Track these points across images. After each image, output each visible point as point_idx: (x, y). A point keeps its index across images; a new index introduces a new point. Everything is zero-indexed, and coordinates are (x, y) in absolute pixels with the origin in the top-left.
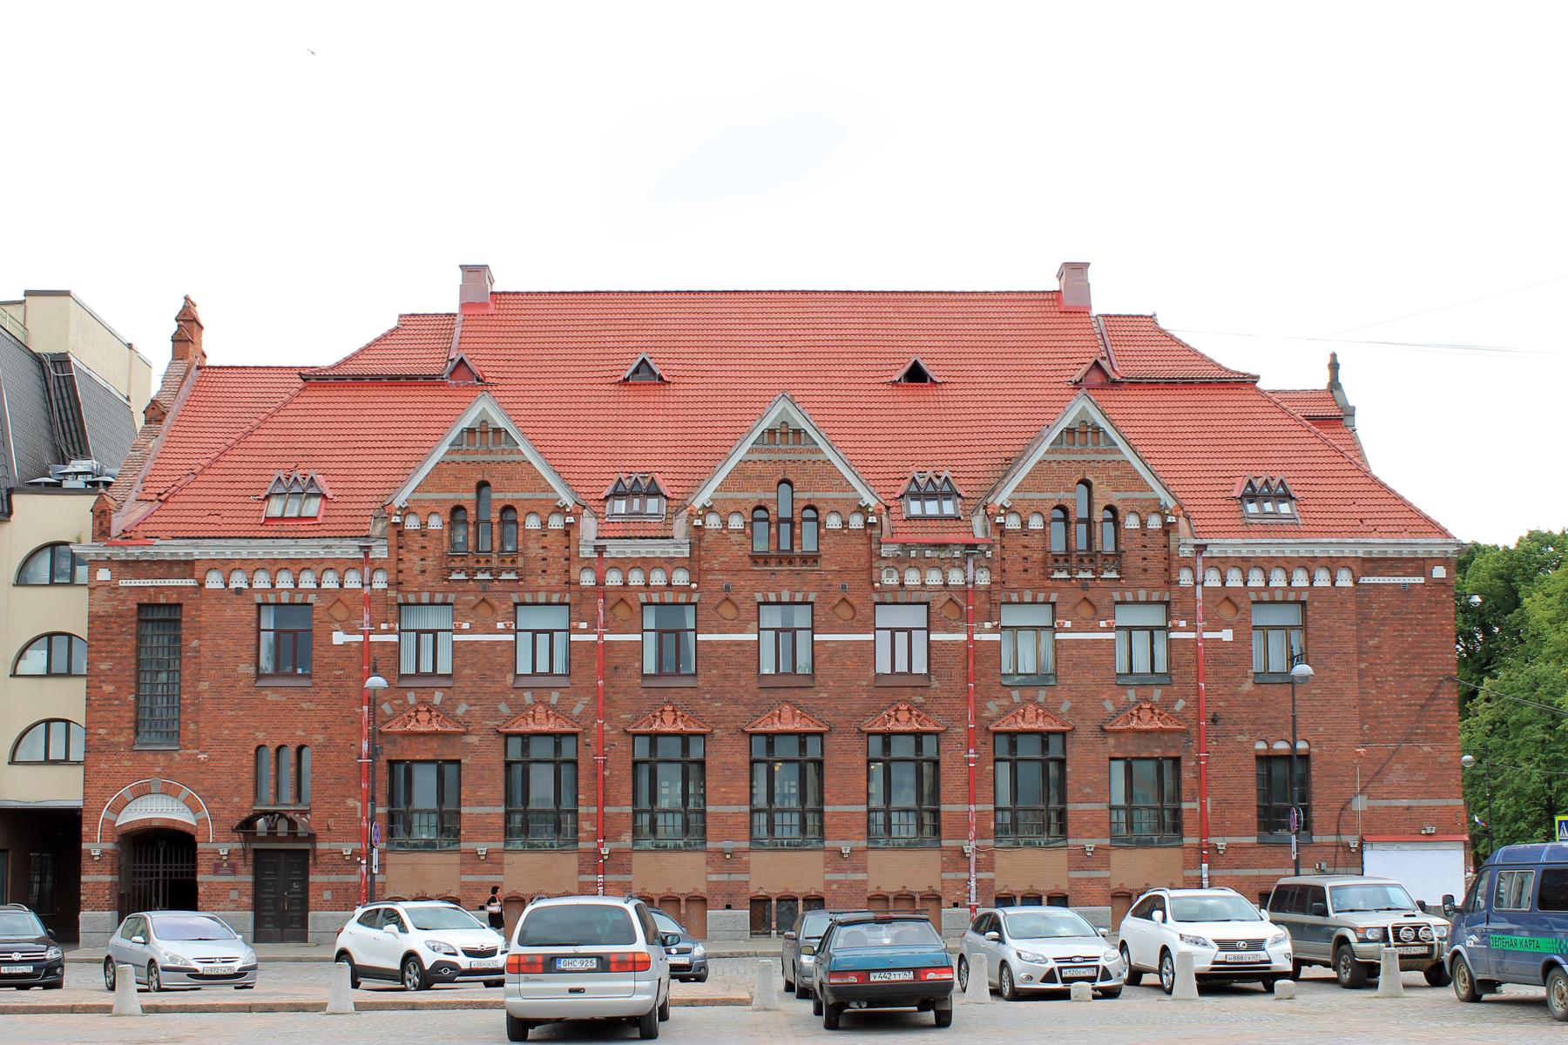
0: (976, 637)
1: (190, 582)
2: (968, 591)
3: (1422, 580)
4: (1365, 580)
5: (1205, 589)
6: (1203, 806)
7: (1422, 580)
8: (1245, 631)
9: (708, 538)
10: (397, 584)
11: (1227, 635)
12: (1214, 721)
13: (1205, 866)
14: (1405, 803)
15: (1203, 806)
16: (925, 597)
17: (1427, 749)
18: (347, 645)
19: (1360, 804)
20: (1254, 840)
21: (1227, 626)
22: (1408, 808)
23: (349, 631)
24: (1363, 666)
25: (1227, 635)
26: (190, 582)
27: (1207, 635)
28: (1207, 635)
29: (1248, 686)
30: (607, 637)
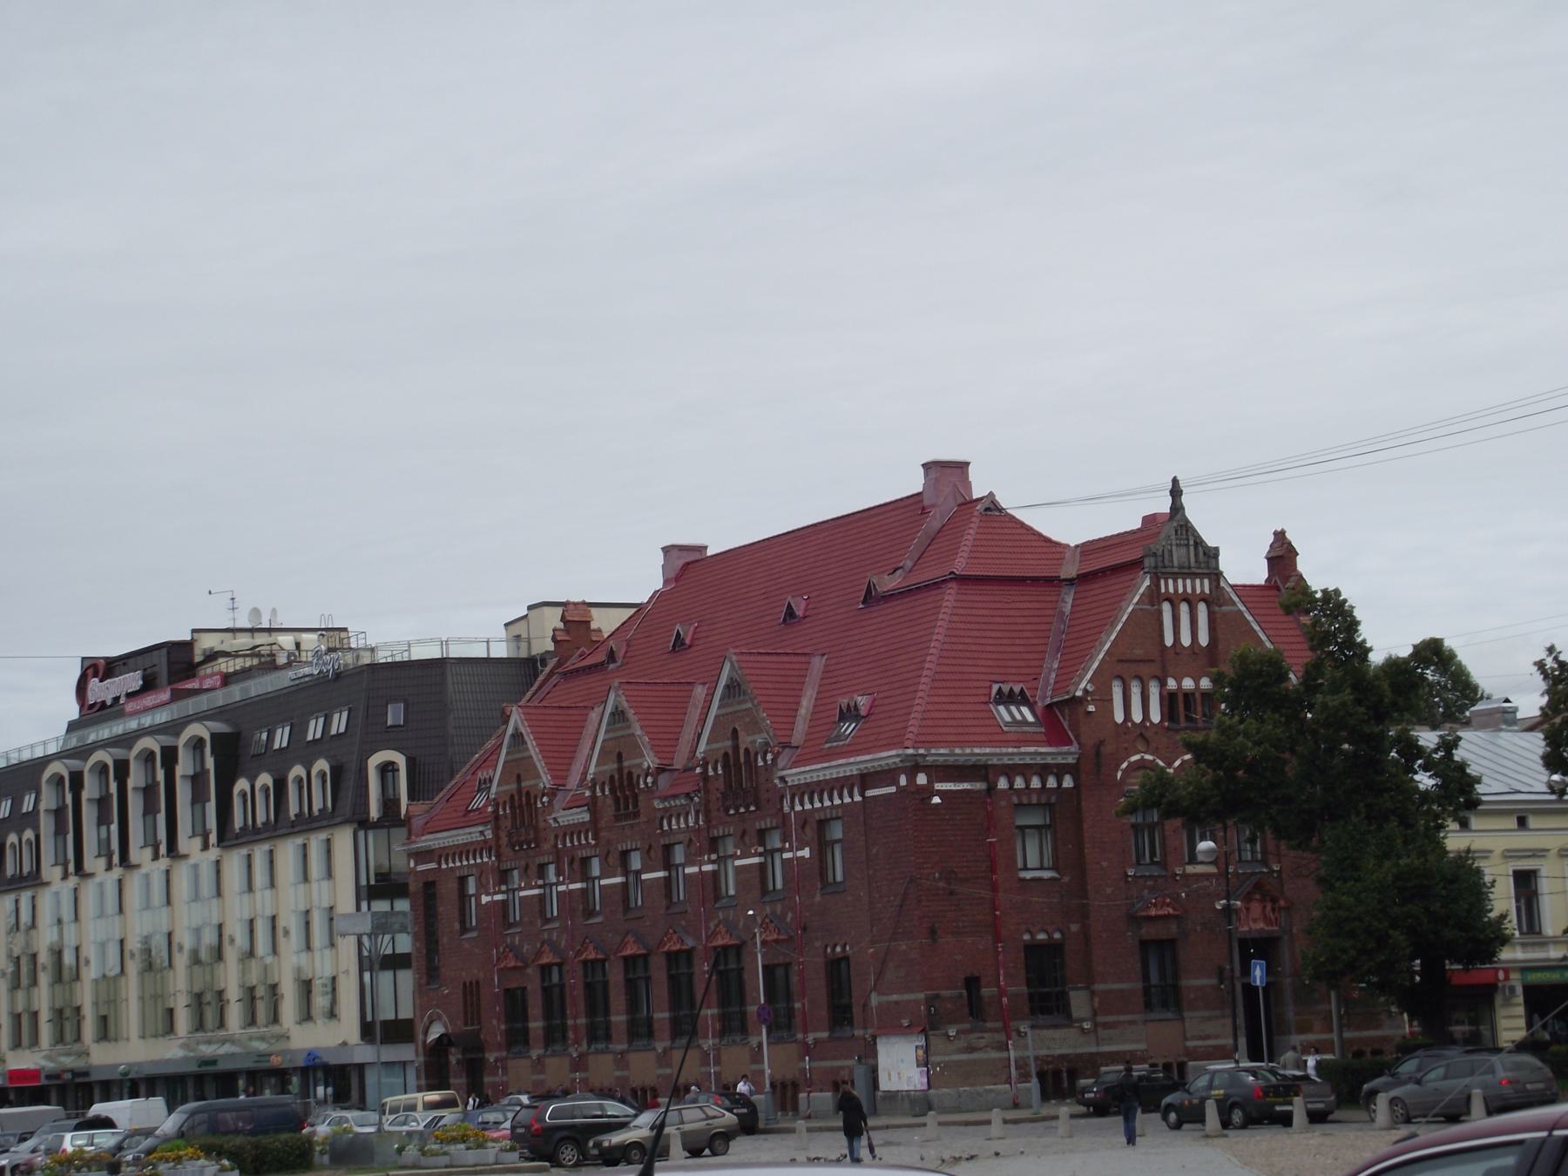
0: (708, 868)
1: (433, 865)
2: (698, 831)
3: (893, 789)
4: (870, 793)
5: (797, 813)
6: (803, 1005)
7: (893, 789)
8: (822, 847)
9: (599, 804)
10: (498, 856)
11: (806, 853)
12: (805, 929)
13: (807, 1058)
14: (895, 997)
15: (803, 1005)
16: (680, 837)
17: (904, 947)
18: (487, 903)
19: (875, 1000)
20: (825, 1035)
21: (807, 844)
22: (897, 1003)
23: (488, 894)
24: (871, 872)
25: (806, 853)
26: (433, 865)
27: (800, 854)
28: (800, 854)
29: (818, 898)
30: (572, 887)
